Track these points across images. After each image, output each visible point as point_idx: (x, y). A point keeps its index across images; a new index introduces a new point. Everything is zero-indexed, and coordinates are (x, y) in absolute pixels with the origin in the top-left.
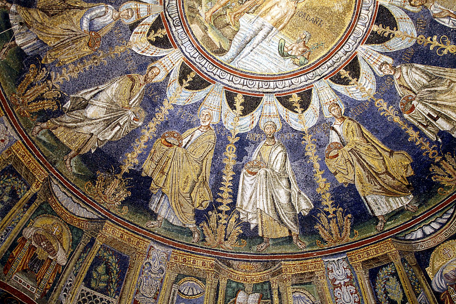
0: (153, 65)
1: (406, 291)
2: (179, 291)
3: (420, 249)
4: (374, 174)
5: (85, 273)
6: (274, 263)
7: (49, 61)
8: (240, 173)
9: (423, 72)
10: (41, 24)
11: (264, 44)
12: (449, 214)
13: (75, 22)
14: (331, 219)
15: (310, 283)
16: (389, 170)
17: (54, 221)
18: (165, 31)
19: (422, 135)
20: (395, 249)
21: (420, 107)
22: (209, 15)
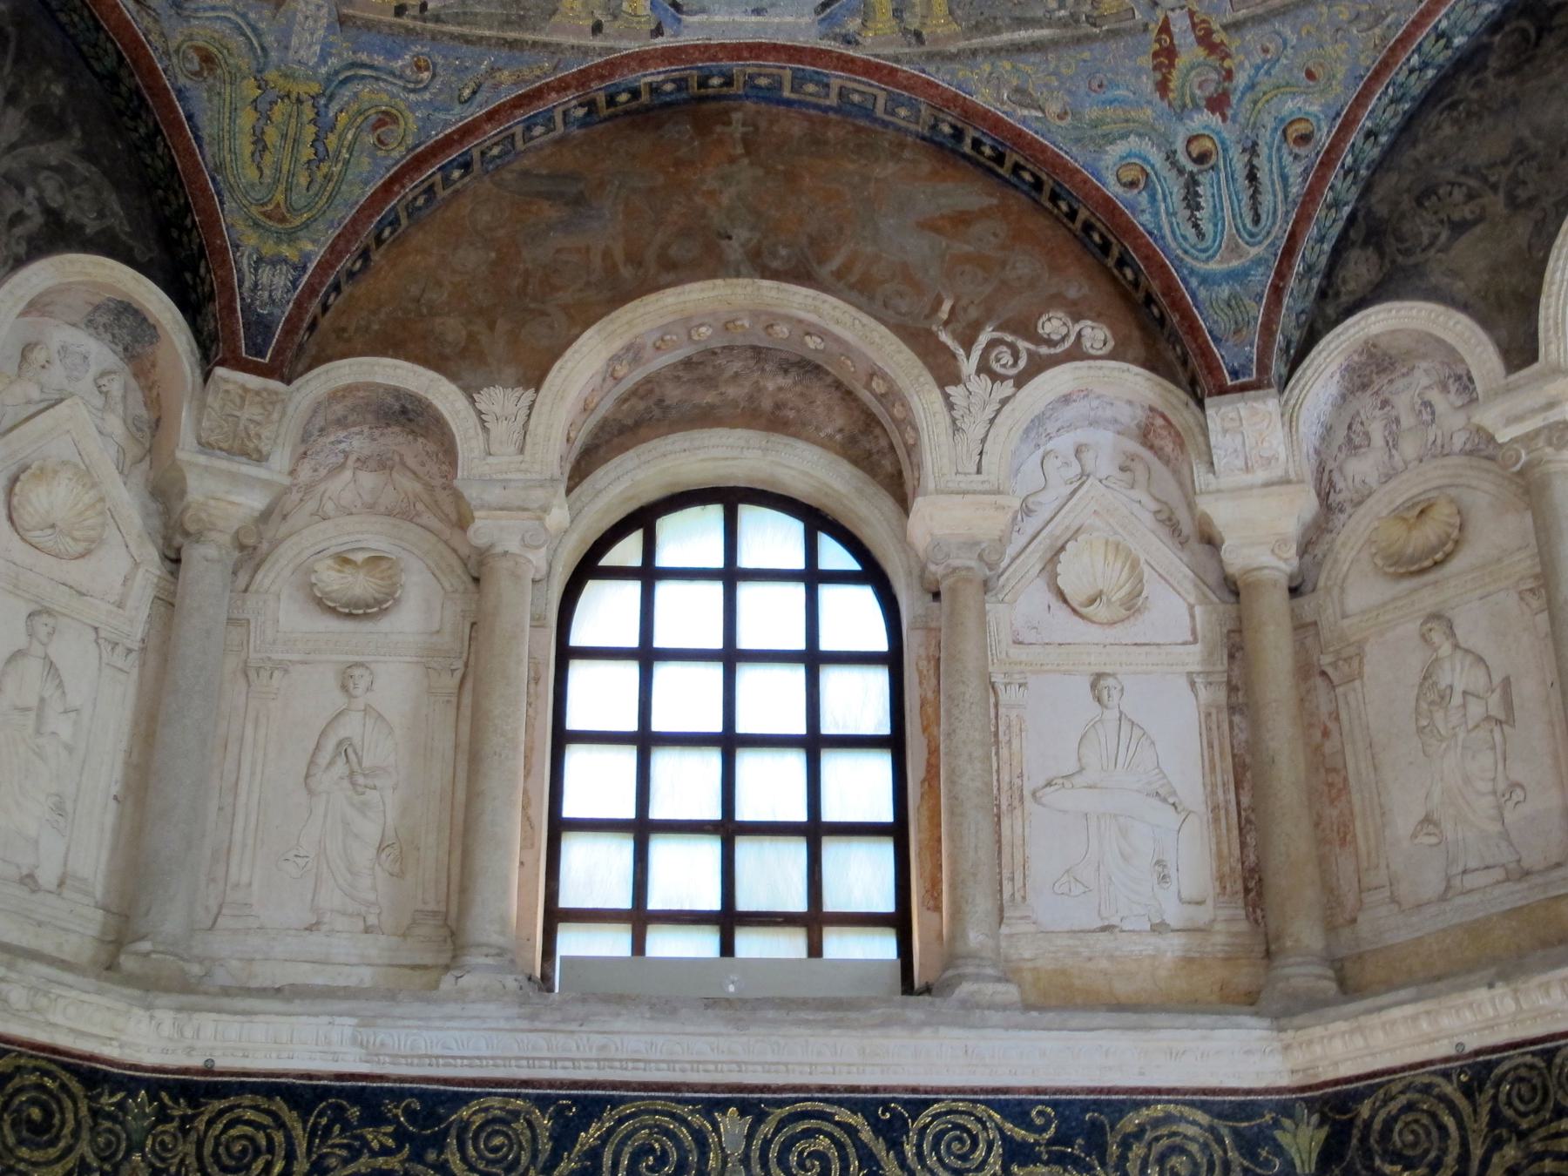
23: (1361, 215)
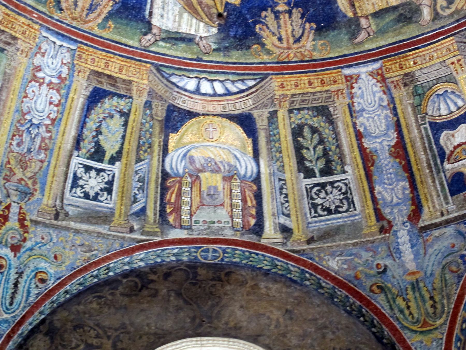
1: (126, 146)
12: (246, 85)
20: (146, 82)
23: (47, 322)
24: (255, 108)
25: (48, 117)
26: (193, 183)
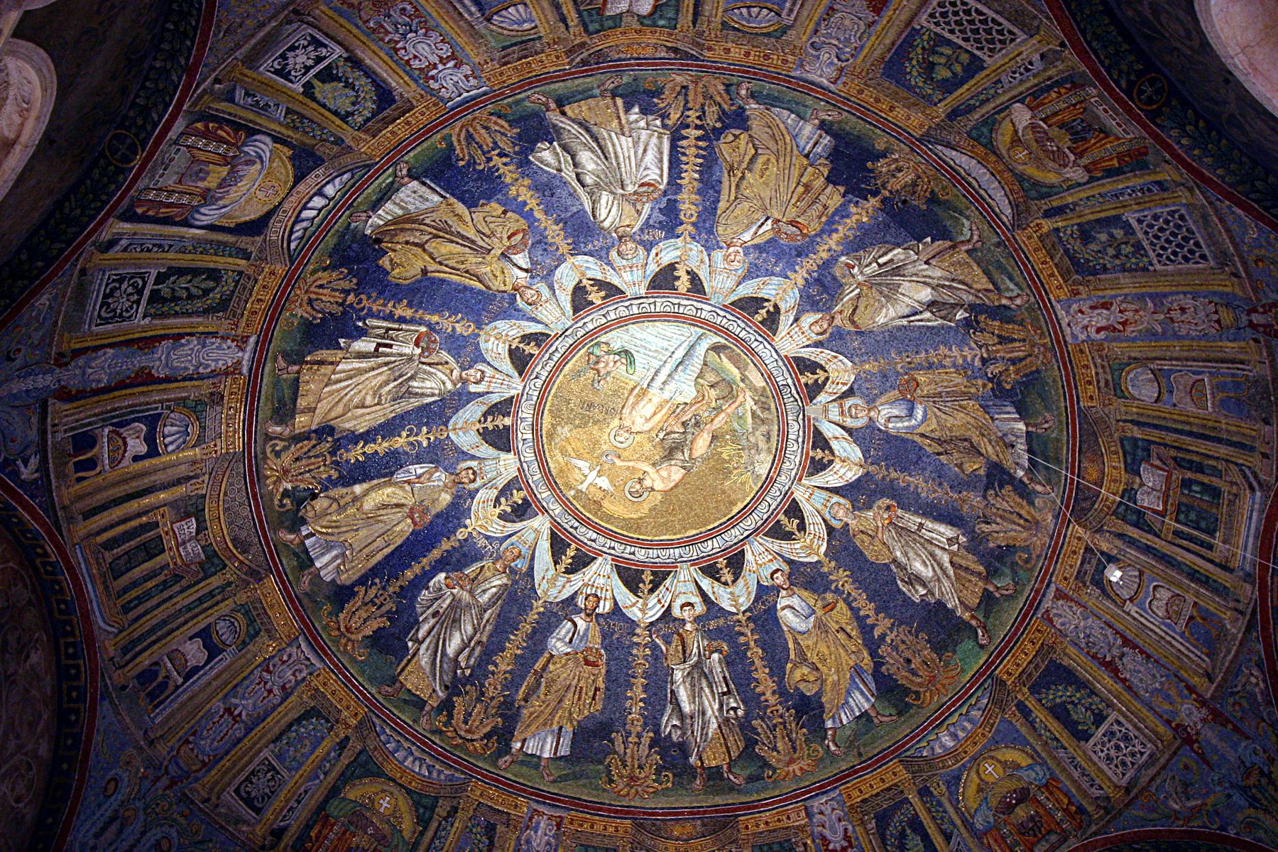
0: (820, 338)
2: (779, 15)
3: (320, 171)
4: (441, 234)
5: (978, 77)
6: (584, 62)
7: (980, 382)
8: (668, 183)
9: (423, 395)
10: (983, 435)
11: (656, 364)
12: (297, 238)
13: (934, 420)
14: (493, 149)
15: (504, 48)
16: (420, 250)
17: (1021, 168)
18: (803, 381)
19: (390, 317)
21: (407, 350)
22: (741, 399)
24: (265, 241)
25: (405, 48)
26: (224, 157)
